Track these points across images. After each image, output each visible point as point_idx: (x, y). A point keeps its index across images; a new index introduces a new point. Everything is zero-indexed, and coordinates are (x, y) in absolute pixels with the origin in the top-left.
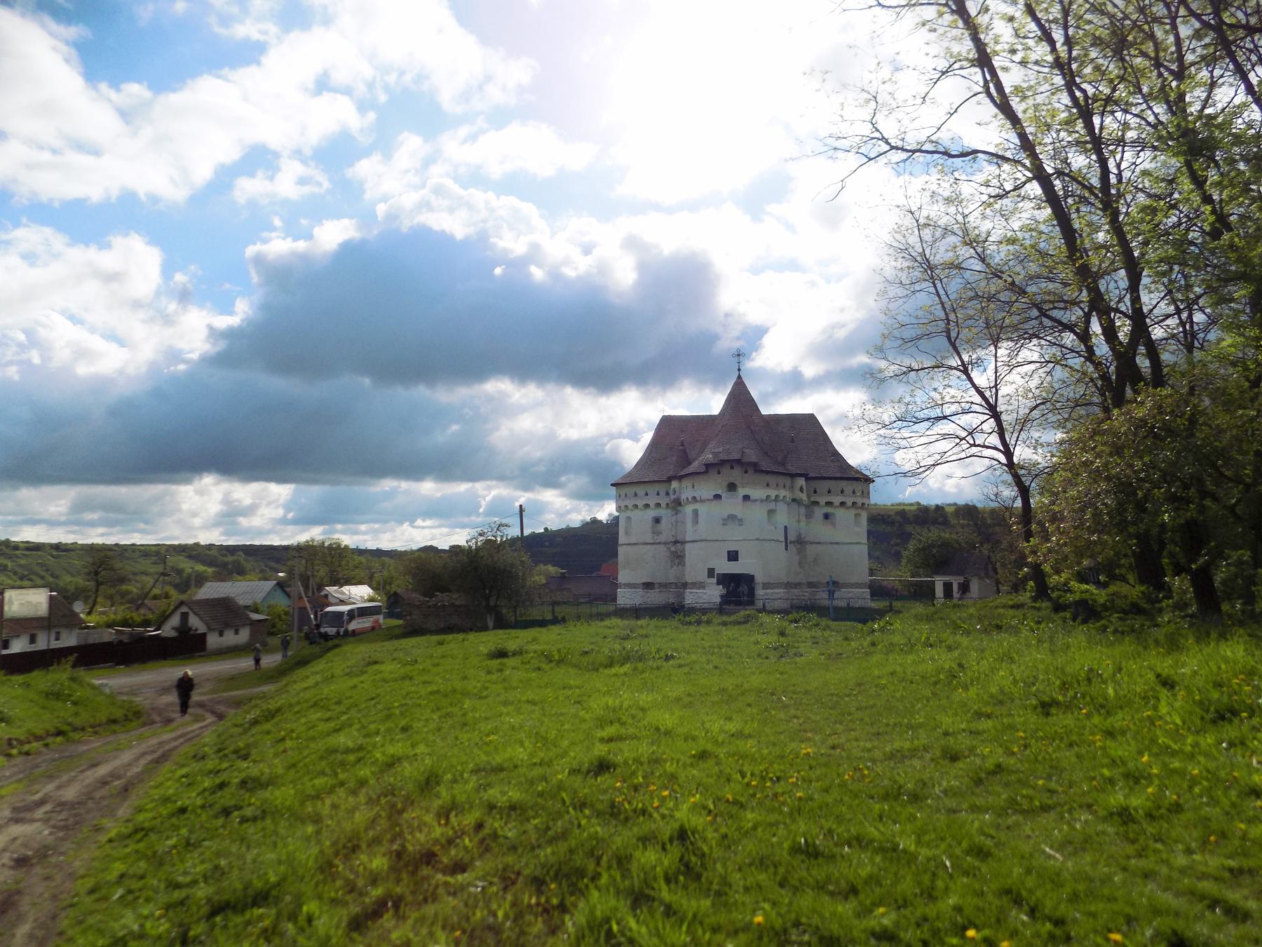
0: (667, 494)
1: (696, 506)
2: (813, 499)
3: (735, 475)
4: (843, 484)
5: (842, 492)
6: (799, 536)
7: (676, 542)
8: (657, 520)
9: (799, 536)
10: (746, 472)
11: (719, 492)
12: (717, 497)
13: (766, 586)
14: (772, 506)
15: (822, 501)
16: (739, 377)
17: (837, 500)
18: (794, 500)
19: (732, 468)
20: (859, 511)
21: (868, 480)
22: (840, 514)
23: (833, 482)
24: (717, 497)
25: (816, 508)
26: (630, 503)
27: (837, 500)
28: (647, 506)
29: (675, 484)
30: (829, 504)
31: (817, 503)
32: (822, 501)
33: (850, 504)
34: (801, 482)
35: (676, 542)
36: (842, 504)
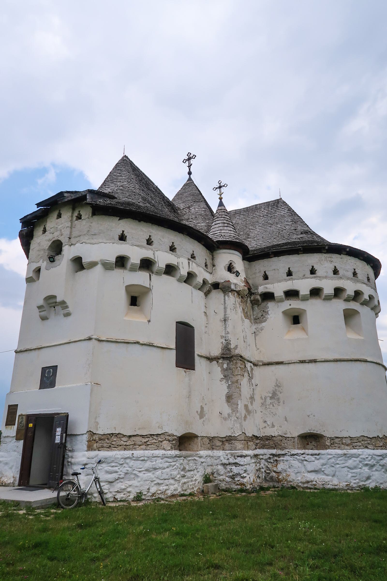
2: (261, 289)
3: (58, 226)
4: (313, 259)
5: (313, 271)
6: (227, 348)
9: (227, 348)
10: (79, 217)
13: (96, 441)
14: (141, 278)
16: (190, 179)
18: (216, 286)
19: (59, 216)
20: (354, 305)
21: (375, 265)
22: (313, 309)
25: (271, 305)
27: (304, 286)
30: (291, 294)
31: (268, 296)
32: (278, 288)
33: (328, 290)
34: (236, 258)
36: (316, 292)
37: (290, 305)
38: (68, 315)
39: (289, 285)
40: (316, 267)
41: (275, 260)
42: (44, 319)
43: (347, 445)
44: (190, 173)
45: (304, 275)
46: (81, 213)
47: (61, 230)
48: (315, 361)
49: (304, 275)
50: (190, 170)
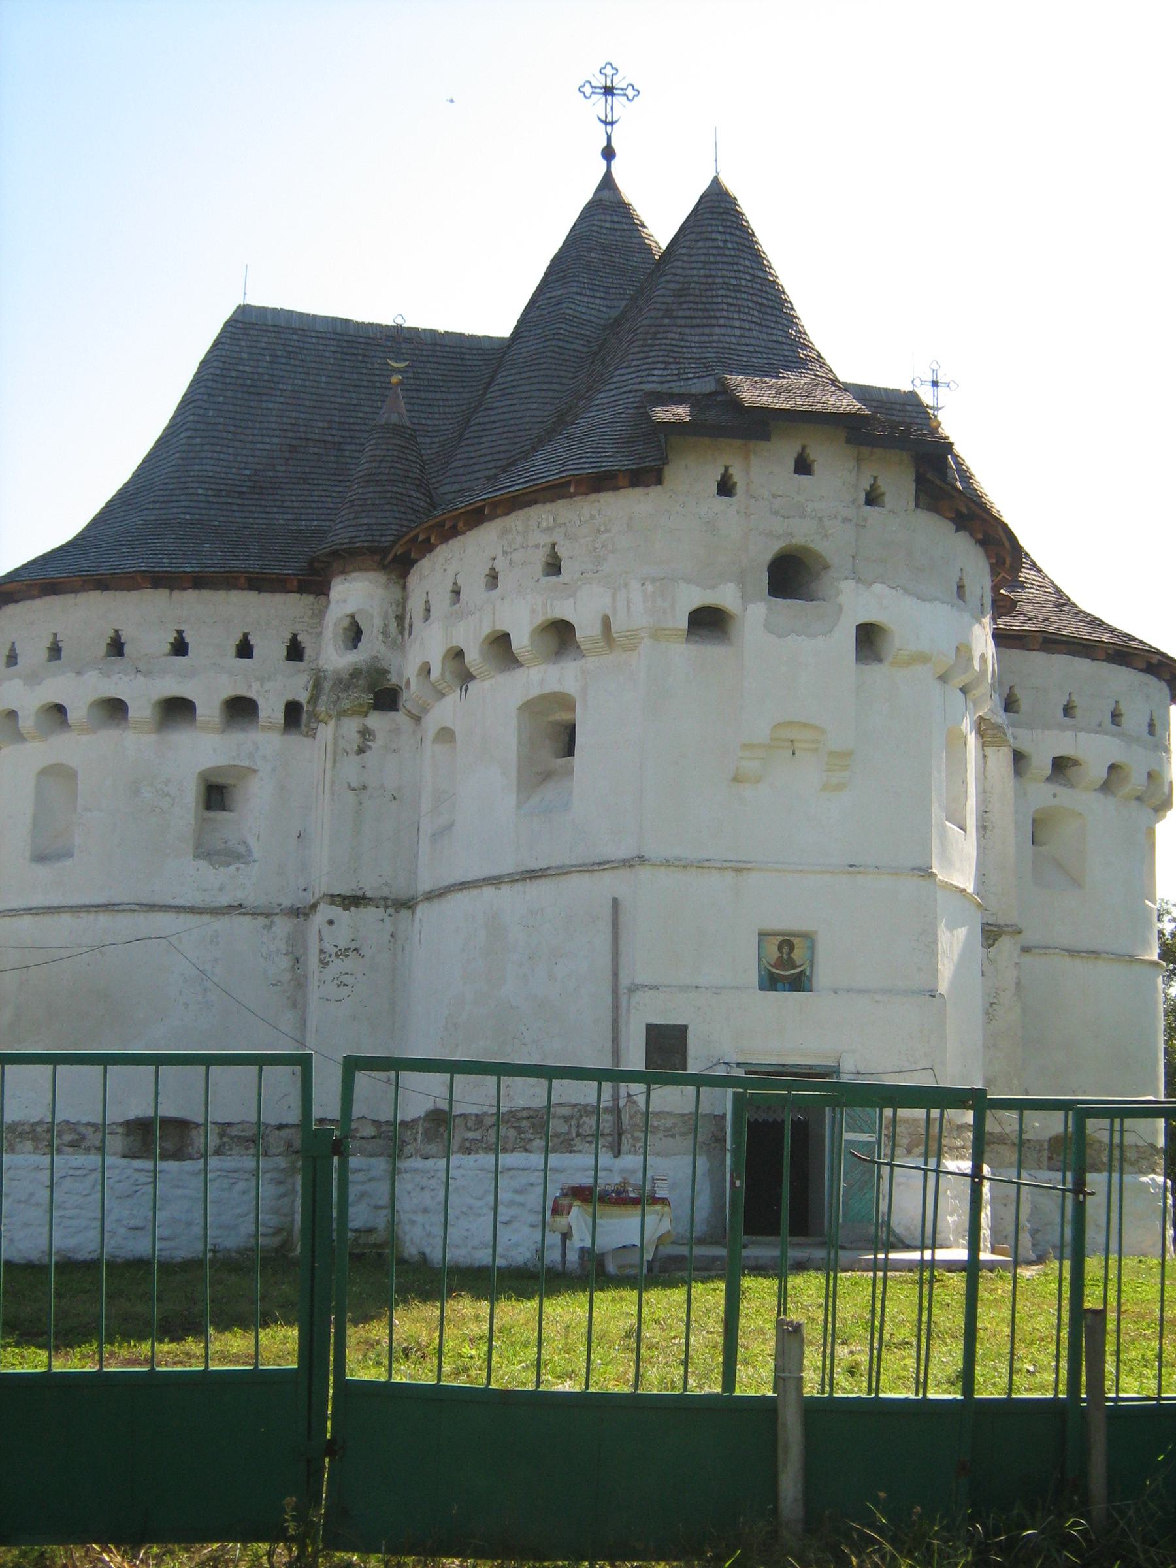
0: (295, 652)
1: (562, 677)
5: (1116, 717)
7: (353, 901)
8: (216, 794)
10: (872, 499)
11: (726, 597)
12: (708, 622)
15: (1046, 745)
16: (608, 183)
17: (1095, 751)
19: (803, 466)
23: (1082, 665)
24: (708, 622)
26: (79, 690)
27: (1095, 751)
28: (176, 710)
29: (355, 593)
30: (1061, 766)
35: (353, 901)
37: (1055, 796)
38: (840, 787)
39: (1063, 743)
40: (1123, 707)
41: (1038, 659)
42: (736, 779)
43: (1132, 1164)
44: (608, 154)
45: (1100, 725)
46: (883, 485)
47: (820, 519)
48: (1095, 954)
49: (1100, 725)
50: (609, 138)
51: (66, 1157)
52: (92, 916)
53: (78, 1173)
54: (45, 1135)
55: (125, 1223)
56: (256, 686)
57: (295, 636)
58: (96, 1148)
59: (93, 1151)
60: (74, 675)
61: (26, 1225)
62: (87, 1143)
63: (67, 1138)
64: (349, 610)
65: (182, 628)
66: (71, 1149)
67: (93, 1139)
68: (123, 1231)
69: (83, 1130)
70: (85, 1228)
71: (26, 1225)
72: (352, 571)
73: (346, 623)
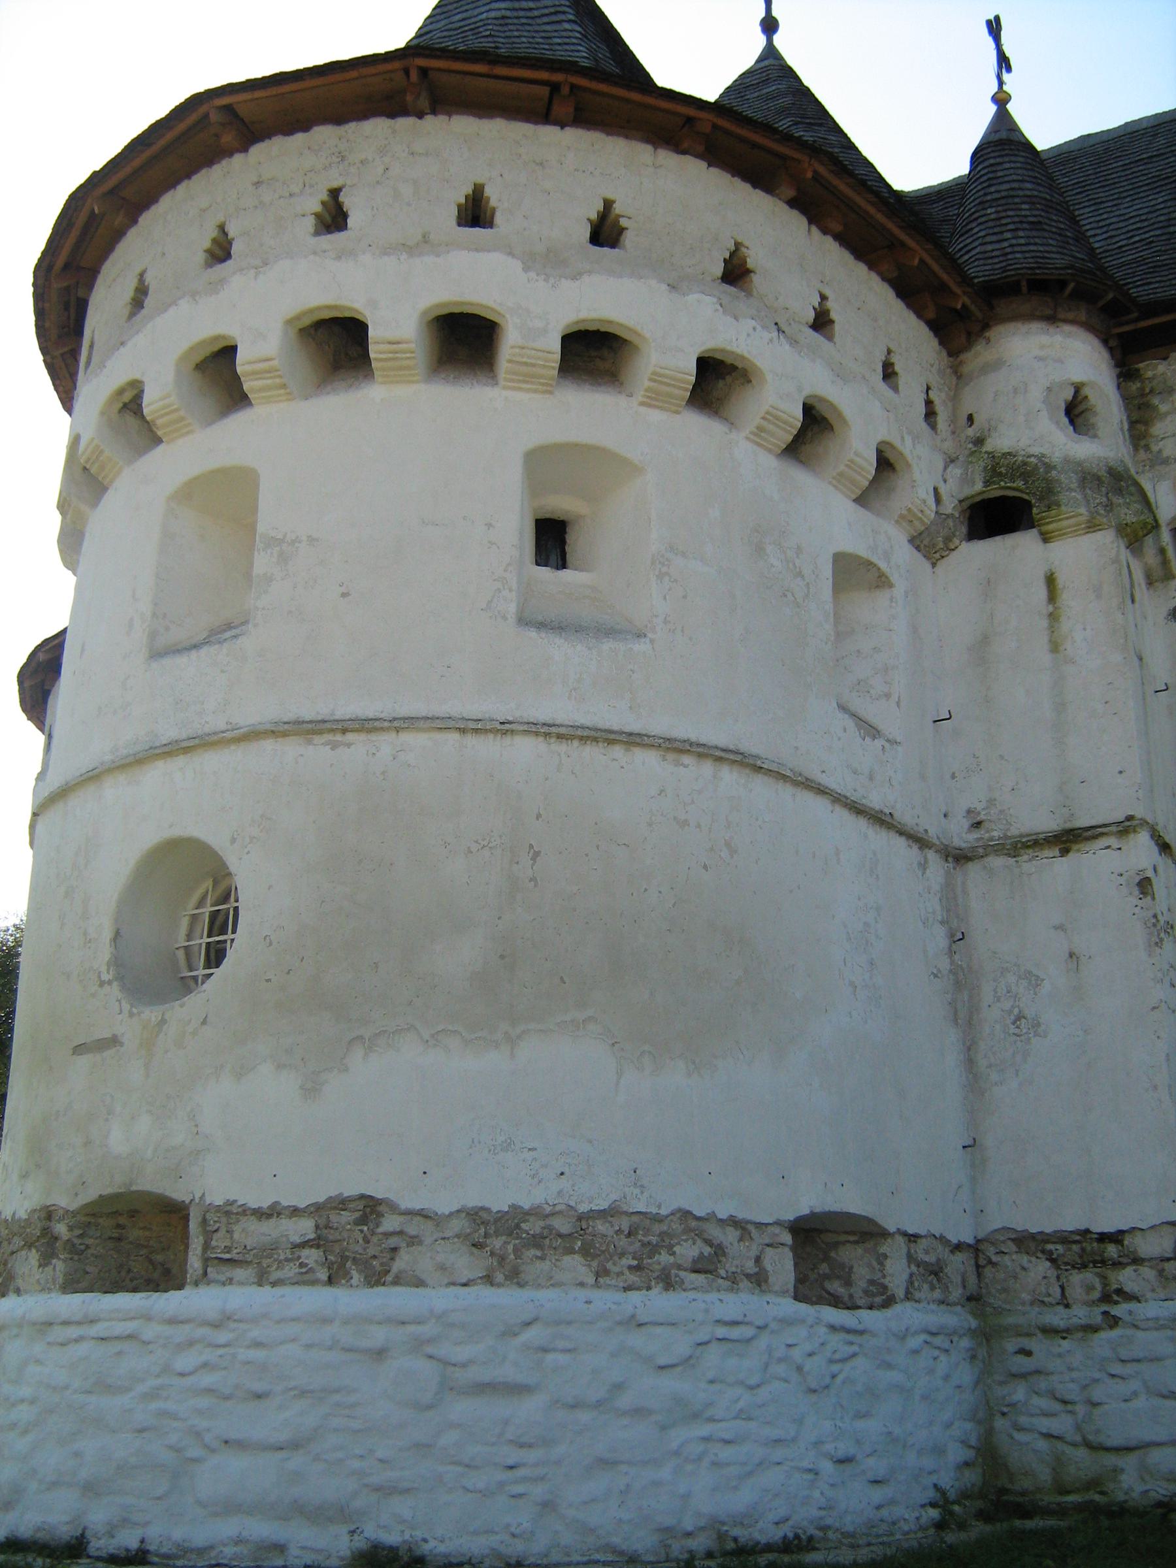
0: (930, 414)
44: (770, 25)
51: (691, 1295)
52: (707, 767)
53: (735, 1333)
54: (623, 1242)
55: (829, 1447)
56: (908, 441)
57: (928, 388)
58: (748, 1276)
59: (745, 1284)
60: (664, 287)
61: (605, 1463)
62: (729, 1266)
63: (688, 1251)
64: (1077, 378)
65: (827, 292)
66: (700, 1279)
67: (741, 1255)
68: (827, 1467)
69: (715, 1232)
70: (760, 1464)
71: (605, 1463)
72: (1066, 321)
73: (1069, 394)
